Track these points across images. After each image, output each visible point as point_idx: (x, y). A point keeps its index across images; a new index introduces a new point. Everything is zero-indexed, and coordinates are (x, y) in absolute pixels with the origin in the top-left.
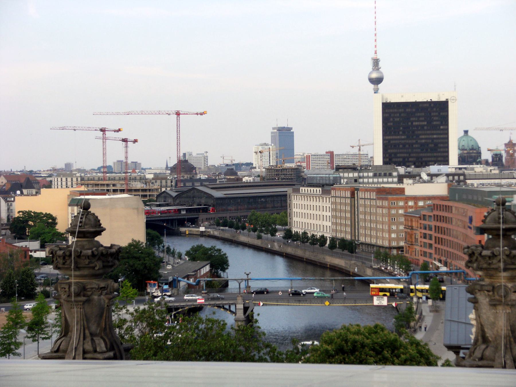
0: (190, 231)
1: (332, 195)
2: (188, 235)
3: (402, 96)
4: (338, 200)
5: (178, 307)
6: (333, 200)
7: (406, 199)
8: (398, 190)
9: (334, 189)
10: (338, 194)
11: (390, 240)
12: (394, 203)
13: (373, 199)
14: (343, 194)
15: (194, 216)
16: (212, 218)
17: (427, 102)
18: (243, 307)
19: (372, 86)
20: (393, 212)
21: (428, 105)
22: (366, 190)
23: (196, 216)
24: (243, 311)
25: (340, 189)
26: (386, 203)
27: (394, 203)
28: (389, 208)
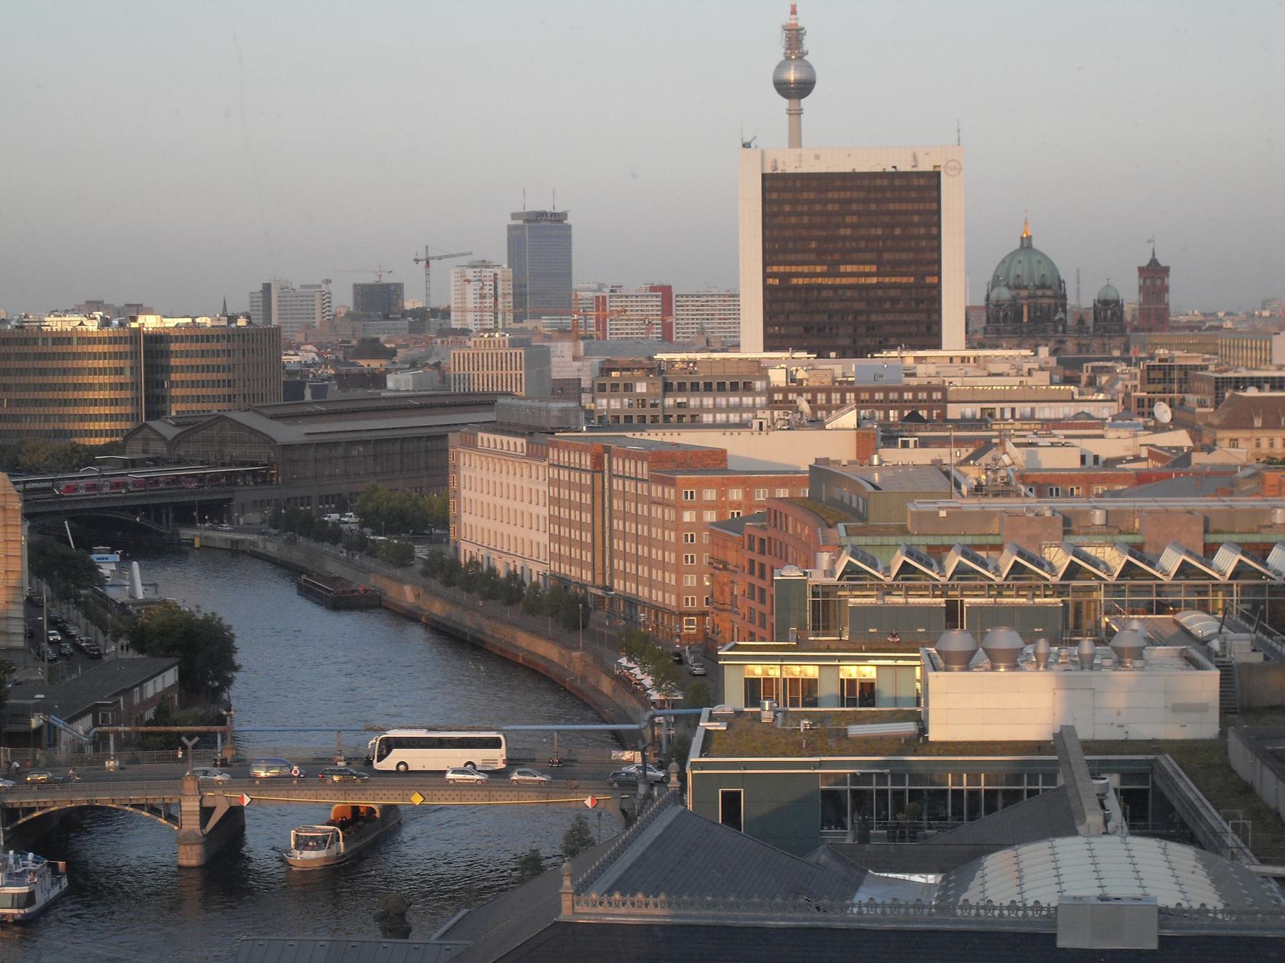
0: (206, 538)
1: (551, 462)
2: (198, 549)
3: (817, 157)
4: (564, 475)
5: (32, 805)
6: (554, 473)
7: (723, 485)
8: (709, 456)
9: (555, 445)
10: (564, 457)
11: (679, 591)
12: (692, 493)
13: (642, 480)
14: (575, 459)
15: (220, 497)
16: (269, 501)
17: (883, 175)
18: (198, 809)
19: (784, 103)
20: (688, 516)
21: (885, 182)
22: (628, 455)
23: (226, 496)
24: (198, 818)
25: (567, 447)
26: (670, 493)
27: (692, 493)
28: (679, 507)
